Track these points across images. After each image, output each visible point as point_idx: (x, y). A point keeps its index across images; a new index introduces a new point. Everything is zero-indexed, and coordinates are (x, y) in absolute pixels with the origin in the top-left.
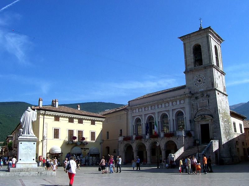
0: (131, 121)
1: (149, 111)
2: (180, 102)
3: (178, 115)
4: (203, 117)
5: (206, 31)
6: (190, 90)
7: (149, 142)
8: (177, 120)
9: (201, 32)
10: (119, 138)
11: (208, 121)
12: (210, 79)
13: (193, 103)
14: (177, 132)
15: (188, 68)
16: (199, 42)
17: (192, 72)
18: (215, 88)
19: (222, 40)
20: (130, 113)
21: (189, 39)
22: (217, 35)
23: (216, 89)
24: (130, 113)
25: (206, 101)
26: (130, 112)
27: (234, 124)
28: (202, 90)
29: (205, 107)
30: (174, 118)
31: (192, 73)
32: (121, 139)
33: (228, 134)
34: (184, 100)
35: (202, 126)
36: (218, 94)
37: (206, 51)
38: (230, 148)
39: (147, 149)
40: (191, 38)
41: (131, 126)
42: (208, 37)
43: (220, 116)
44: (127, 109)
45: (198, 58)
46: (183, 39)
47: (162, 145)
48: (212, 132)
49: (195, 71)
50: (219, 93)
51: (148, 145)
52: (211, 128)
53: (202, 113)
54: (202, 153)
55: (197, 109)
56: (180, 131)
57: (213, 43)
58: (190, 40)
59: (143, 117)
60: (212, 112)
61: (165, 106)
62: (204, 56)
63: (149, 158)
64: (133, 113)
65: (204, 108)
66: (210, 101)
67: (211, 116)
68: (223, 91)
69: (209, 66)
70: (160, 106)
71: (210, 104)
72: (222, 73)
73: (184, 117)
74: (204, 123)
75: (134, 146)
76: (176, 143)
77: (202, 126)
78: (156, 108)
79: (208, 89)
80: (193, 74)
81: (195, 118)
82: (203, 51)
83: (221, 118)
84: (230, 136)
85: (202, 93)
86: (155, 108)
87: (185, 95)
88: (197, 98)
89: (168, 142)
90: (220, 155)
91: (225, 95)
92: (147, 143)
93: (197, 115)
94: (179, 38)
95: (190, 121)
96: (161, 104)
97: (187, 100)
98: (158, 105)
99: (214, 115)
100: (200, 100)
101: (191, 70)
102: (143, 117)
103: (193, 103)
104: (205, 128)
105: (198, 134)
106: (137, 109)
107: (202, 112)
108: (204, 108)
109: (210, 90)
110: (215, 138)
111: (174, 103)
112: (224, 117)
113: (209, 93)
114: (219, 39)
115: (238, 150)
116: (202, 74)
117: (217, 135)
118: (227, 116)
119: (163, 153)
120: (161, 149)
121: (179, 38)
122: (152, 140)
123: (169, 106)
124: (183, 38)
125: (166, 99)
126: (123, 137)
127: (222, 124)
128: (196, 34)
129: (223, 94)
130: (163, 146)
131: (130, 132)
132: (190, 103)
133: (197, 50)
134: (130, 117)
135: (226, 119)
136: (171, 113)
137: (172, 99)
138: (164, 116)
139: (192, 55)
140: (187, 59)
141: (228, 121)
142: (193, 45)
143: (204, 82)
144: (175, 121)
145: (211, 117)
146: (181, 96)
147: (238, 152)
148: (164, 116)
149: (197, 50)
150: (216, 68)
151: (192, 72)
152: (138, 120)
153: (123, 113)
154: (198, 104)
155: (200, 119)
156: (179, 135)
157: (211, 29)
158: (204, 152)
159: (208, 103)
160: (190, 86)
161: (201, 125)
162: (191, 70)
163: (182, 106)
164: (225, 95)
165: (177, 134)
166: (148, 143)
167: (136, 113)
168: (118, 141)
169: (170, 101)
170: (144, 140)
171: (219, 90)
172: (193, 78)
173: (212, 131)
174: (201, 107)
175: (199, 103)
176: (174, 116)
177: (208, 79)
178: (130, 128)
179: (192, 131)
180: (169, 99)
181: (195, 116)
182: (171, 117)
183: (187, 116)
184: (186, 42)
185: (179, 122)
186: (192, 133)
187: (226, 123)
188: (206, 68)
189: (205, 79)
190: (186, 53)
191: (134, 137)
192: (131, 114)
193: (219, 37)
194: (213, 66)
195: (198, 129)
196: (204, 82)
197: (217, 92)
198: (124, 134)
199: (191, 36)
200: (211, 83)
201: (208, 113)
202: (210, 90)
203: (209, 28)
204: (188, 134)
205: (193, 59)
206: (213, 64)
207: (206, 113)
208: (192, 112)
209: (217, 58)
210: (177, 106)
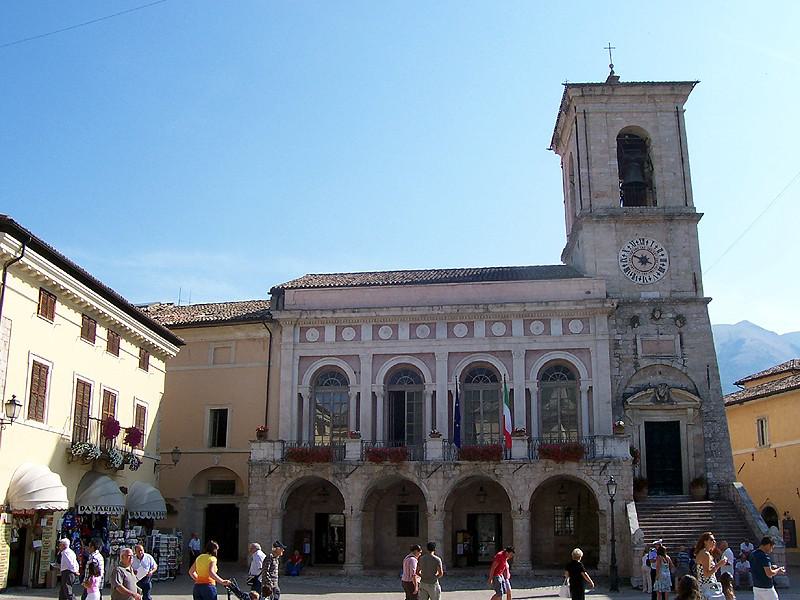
1: (404, 346)
2: (565, 326)
4: (663, 398)
5: (676, 92)
12: (686, 261)
13: (619, 337)
21: (605, 99)
25: (673, 337)
26: (287, 336)
28: (656, 295)
29: (667, 357)
31: (613, 225)
34: (585, 321)
35: (651, 427)
40: (613, 100)
41: (292, 399)
44: (276, 320)
46: (583, 96)
48: (692, 454)
49: (627, 223)
52: (688, 437)
55: (636, 365)
58: (609, 106)
60: (698, 378)
61: (490, 335)
62: (662, 177)
64: (303, 340)
65: (664, 362)
66: (685, 341)
71: (687, 351)
74: (660, 417)
77: (651, 427)
78: (442, 333)
79: (679, 295)
80: (616, 231)
82: (661, 157)
85: (657, 307)
88: (634, 321)
92: (433, 480)
97: (602, 324)
98: (450, 326)
100: (648, 328)
102: (366, 367)
103: (619, 337)
107: (654, 375)
108: (664, 362)
109: (686, 301)
113: (682, 309)
117: (716, 465)
133: (633, 150)
136: (518, 364)
137: (529, 308)
145: (693, 396)
156: (610, 457)
159: (682, 348)
161: (648, 424)
163: (572, 342)
166: (441, 481)
167: (327, 347)
168: (251, 464)
170: (418, 468)
173: (691, 448)
174: (652, 357)
177: (678, 262)
180: (518, 309)
200: (691, 277)
202: (686, 301)
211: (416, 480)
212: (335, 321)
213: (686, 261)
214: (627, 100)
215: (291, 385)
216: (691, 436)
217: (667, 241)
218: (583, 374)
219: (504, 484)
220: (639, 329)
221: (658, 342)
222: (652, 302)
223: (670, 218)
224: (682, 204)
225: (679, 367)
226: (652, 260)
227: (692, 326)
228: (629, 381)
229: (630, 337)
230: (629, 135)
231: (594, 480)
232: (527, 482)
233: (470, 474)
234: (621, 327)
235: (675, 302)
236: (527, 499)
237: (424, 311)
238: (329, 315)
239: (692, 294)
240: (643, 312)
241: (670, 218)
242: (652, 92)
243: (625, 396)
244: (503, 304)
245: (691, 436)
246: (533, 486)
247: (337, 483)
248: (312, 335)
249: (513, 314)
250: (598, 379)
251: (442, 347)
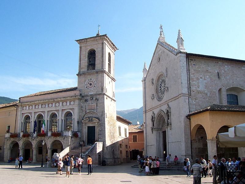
0: (20, 117)
3: (67, 116)
5: (102, 38)
6: (80, 92)
7: (36, 141)
8: (66, 120)
9: (97, 38)
10: (6, 134)
11: (95, 123)
12: (100, 84)
13: (83, 105)
14: (64, 132)
15: (81, 71)
16: (94, 47)
17: (85, 75)
18: (104, 92)
19: (116, 48)
20: (20, 109)
22: (112, 43)
23: (104, 94)
24: (20, 109)
25: (95, 104)
26: (20, 109)
27: (120, 128)
28: (92, 93)
29: (93, 110)
30: (63, 118)
32: (7, 135)
33: (112, 136)
35: (89, 128)
36: (107, 98)
38: (113, 150)
41: (20, 123)
42: (103, 44)
43: (106, 119)
45: (92, 62)
47: (48, 144)
50: (108, 98)
51: (34, 143)
52: (97, 130)
53: (90, 115)
54: (85, 154)
55: (86, 112)
56: (67, 131)
57: (108, 49)
59: (33, 115)
60: (99, 115)
62: (98, 62)
63: (34, 156)
64: (23, 110)
65: (92, 111)
67: (98, 118)
68: (111, 97)
69: (101, 71)
70: (50, 105)
72: (113, 79)
73: (73, 118)
74: (91, 125)
75: (21, 143)
76: (62, 143)
77: (89, 128)
78: (47, 106)
79: (97, 93)
81: (83, 119)
83: (108, 122)
84: (114, 139)
85: (92, 97)
86: (45, 107)
87: (76, 96)
88: (86, 101)
89: (55, 141)
90: (103, 157)
91: (113, 100)
92: (34, 141)
93: (86, 116)
94: (76, 41)
95: (78, 122)
96: (52, 104)
97: (77, 102)
98: (48, 104)
99: (101, 119)
100: (90, 102)
101: (84, 74)
102: (33, 115)
103: (83, 105)
104: (91, 130)
105: (85, 135)
106: (28, 107)
107: (90, 114)
108: (92, 111)
110: (100, 140)
111: (65, 103)
112: (110, 120)
113: (98, 97)
114: (114, 47)
115: (120, 152)
116: (93, 78)
117: (101, 137)
118: (113, 120)
119: (49, 152)
120: (48, 148)
121: (77, 41)
122: (39, 138)
123: (59, 106)
124: (80, 41)
125: (57, 99)
126: (10, 134)
127: (108, 127)
129: (112, 99)
130: (50, 145)
131: (18, 129)
132: (79, 105)
133: (92, 54)
134: (19, 114)
135: (112, 123)
138: (54, 116)
139: (87, 59)
140: (81, 62)
141: (114, 126)
143: (95, 86)
144: (63, 121)
145: (98, 120)
146: (71, 97)
147: (121, 153)
148: (54, 116)
149: (92, 54)
150: (107, 74)
151: (85, 75)
152: (28, 118)
153: (13, 109)
154: (87, 106)
155: (87, 122)
157: (107, 37)
158: (87, 152)
159: (97, 107)
160: (81, 88)
162: (84, 74)
163: (71, 107)
164: (113, 100)
165: (64, 134)
167: (27, 111)
168: (5, 138)
169: (61, 101)
170: (31, 138)
171: (108, 95)
174: (90, 110)
175: (88, 105)
176: (63, 116)
177: (98, 84)
178: (19, 126)
179: (79, 132)
181: (83, 117)
182: (60, 117)
183: (75, 117)
184: (82, 45)
185: (67, 122)
186: (79, 134)
187: (111, 127)
188: (98, 73)
189: (96, 83)
190: (81, 56)
191: (22, 134)
192: (21, 110)
193: (114, 45)
194: (104, 72)
195: (85, 130)
196: (95, 86)
197: (105, 97)
198: (12, 131)
199: (88, 40)
200: (101, 88)
201: (96, 116)
203: (105, 35)
204: (75, 135)
205: (87, 62)
206: (105, 70)
207: (94, 116)
208: (81, 114)
209: (109, 65)
210: (67, 107)
212: (35, 104)
215: (20, 120)
216: (97, 130)
218: (73, 114)
221: (91, 106)
222: (91, 95)
224: (101, 68)
225: (96, 112)
227: (100, 101)
230: (93, 51)
234: (84, 102)
235: (96, 95)
237: (38, 102)
238: (26, 103)
240: (88, 98)
245: (97, 130)
248: (24, 108)
251: (47, 109)
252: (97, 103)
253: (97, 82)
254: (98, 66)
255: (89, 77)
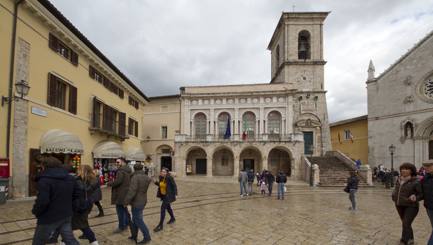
12: (319, 78)
16: (309, 29)
21: (296, 19)
37: (317, 42)
39: (235, 155)
40: (298, 20)
47: (264, 152)
55: (300, 113)
62: (313, 49)
66: (317, 105)
71: (317, 108)
85: (308, 94)
88: (301, 98)
92: (236, 147)
100: (305, 100)
102: (212, 113)
109: (318, 92)
113: (317, 95)
128: (307, 17)
138: (249, 115)
142: (299, 31)
143: (310, 82)
154: (301, 105)
166: (239, 148)
172: (297, 73)
196: (310, 82)
202: (318, 92)
211: (230, 147)
213: (319, 78)
214: (303, 20)
217: (313, 71)
219: (260, 149)
220: (302, 101)
222: (307, 92)
223: (315, 63)
225: (315, 114)
226: (307, 79)
227: (319, 100)
228: (297, 118)
229: (299, 104)
231: (289, 147)
232: (267, 148)
233: (248, 145)
234: (296, 101)
235: (314, 92)
236: (268, 154)
239: (320, 90)
241: (315, 63)
242: (313, 16)
243: (298, 122)
244: (258, 92)
246: (270, 150)
247: (205, 149)
249: (260, 95)
250: (289, 116)
252: (316, 103)
253: (315, 76)
254: (314, 57)
255: (302, 68)
